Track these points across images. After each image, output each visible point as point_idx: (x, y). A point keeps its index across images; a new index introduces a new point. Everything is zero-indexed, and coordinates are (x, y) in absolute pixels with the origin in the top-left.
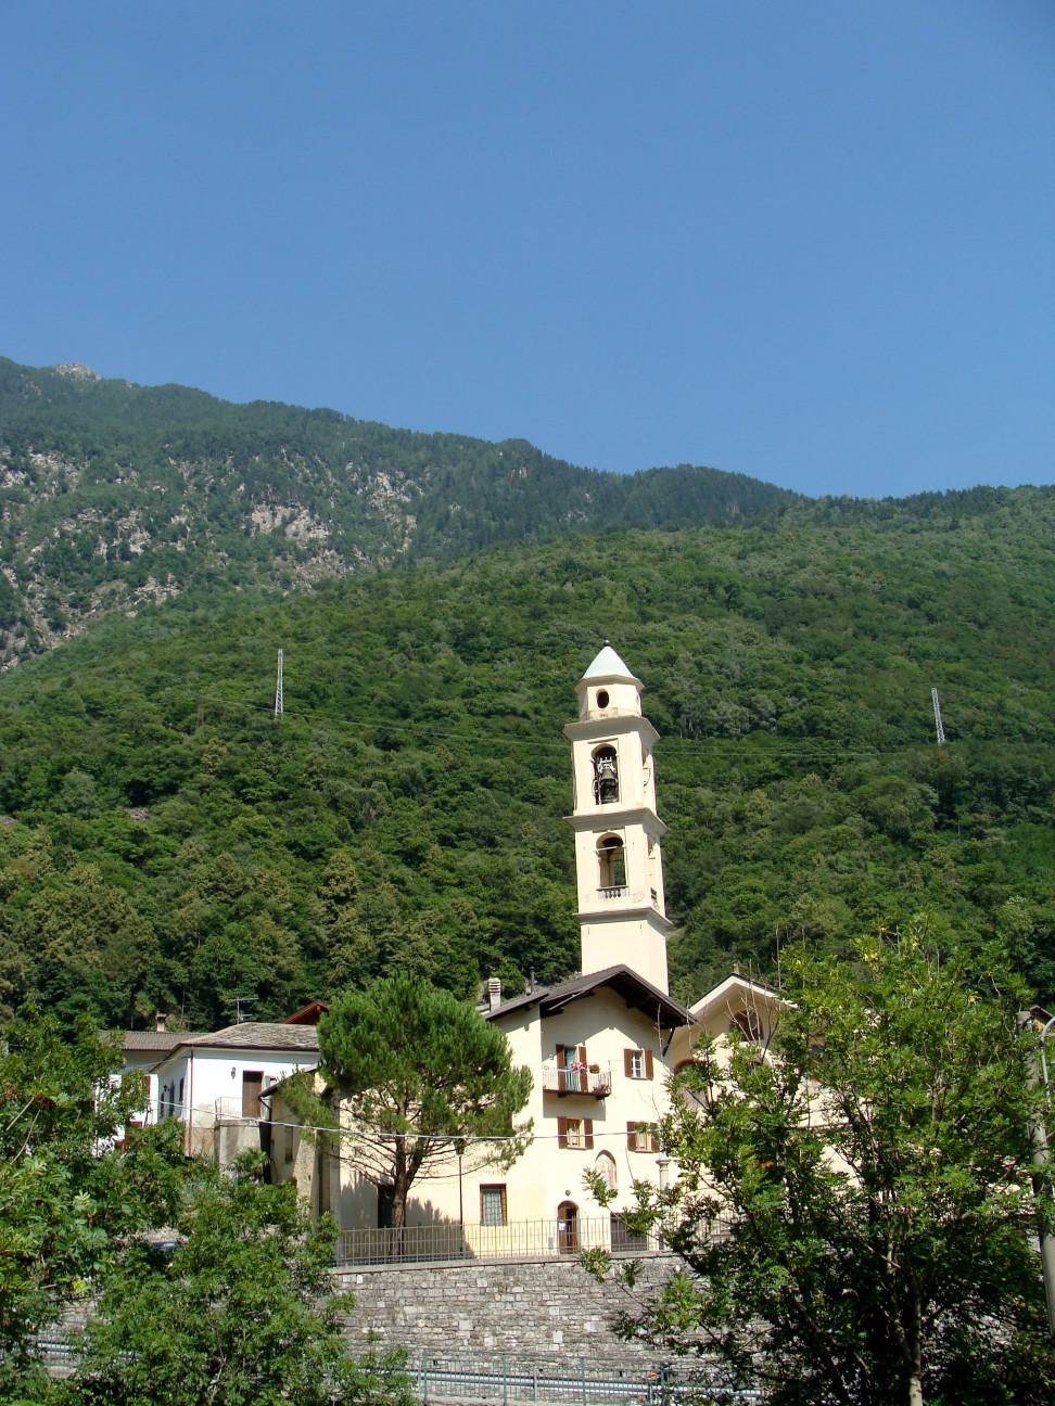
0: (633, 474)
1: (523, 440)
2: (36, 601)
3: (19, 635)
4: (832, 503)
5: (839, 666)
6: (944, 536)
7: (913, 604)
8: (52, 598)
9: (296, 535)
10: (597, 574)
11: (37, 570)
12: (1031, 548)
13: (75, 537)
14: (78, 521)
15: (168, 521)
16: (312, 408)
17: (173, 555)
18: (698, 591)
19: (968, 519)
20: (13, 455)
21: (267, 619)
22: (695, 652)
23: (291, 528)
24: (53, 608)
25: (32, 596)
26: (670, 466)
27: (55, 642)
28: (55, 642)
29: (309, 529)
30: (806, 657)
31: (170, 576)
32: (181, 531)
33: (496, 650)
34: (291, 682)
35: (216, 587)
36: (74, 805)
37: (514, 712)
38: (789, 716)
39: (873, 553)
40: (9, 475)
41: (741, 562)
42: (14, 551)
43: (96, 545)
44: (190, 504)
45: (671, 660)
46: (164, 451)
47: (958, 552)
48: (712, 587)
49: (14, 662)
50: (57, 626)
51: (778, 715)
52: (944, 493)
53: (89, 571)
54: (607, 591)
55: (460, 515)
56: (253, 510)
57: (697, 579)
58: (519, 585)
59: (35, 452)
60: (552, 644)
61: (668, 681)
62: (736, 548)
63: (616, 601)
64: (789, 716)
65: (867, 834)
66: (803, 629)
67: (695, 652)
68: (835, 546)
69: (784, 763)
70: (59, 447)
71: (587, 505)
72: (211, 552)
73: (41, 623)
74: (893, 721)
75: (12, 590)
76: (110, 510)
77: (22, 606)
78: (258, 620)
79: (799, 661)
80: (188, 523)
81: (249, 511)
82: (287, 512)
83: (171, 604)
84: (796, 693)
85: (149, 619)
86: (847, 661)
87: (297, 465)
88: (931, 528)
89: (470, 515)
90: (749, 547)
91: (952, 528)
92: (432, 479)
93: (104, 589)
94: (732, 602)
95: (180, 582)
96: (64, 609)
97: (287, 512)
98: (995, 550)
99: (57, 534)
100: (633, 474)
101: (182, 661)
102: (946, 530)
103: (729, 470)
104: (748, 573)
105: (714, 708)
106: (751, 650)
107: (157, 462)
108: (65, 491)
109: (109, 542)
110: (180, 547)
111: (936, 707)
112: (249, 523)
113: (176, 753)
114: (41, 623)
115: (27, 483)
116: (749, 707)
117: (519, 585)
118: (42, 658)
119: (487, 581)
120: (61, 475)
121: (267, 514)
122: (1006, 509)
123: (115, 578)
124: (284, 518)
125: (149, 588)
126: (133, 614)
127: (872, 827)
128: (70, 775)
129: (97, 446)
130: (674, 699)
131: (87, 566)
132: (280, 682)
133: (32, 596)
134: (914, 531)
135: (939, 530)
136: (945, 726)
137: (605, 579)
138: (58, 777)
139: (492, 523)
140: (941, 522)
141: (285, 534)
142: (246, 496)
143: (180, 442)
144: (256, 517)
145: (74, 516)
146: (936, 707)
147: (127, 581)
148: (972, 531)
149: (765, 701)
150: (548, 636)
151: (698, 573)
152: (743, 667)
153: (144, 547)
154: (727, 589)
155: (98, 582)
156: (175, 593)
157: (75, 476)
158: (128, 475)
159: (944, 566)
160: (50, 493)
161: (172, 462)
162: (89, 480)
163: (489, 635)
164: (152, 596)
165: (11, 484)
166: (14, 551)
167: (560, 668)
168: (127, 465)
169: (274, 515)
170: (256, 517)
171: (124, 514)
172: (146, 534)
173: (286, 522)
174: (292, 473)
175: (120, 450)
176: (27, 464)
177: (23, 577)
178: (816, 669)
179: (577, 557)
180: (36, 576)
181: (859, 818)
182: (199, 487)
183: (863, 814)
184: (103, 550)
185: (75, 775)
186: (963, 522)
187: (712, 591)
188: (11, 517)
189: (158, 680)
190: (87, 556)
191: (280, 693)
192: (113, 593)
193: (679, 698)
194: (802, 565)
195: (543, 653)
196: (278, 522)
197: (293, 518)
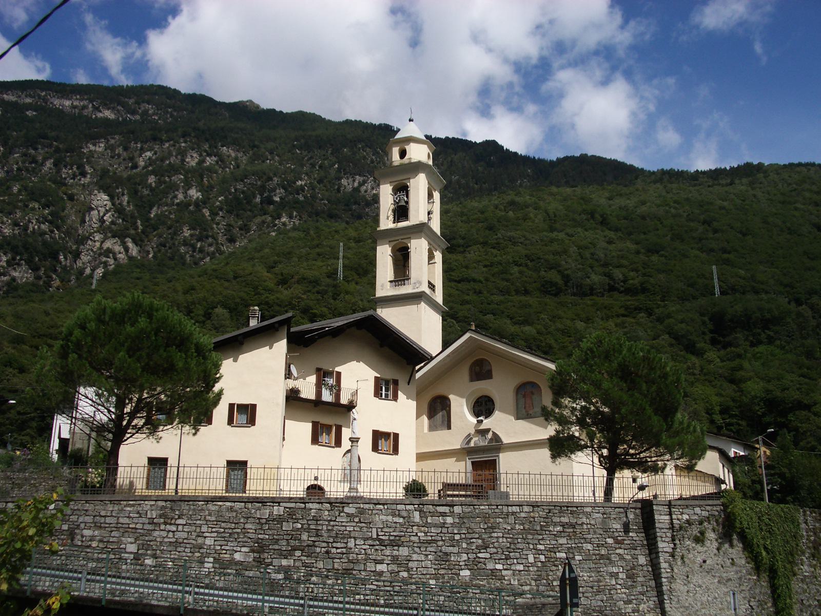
0: (555, 160)
1: (494, 141)
2: (220, 226)
3: (211, 245)
4: (663, 172)
5: (662, 256)
6: (726, 189)
7: (704, 222)
8: (229, 225)
9: (366, 191)
10: (527, 207)
11: (221, 209)
12: (775, 195)
13: (243, 192)
14: (245, 183)
15: (295, 183)
16: (377, 123)
17: (297, 202)
18: (584, 217)
19: (740, 179)
20: (210, 147)
21: (341, 231)
22: (579, 248)
23: (363, 188)
24: (230, 230)
25: (218, 224)
26: (576, 155)
27: (227, 248)
28: (227, 248)
29: (373, 189)
30: (643, 251)
31: (295, 213)
32: (302, 188)
33: (467, 247)
34: (347, 262)
35: (320, 219)
36: (217, 326)
37: (474, 280)
38: (631, 282)
39: (686, 196)
40: (208, 158)
41: (611, 202)
42: (209, 199)
43: (255, 197)
44: (307, 174)
45: (565, 252)
46: (294, 146)
47: (733, 197)
48: (592, 215)
49: (208, 259)
50: (232, 240)
51: (625, 281)
52: (728, 168)
53: (250, 211)
54: (532, 215)
55: (458, 182)
56: (342, 178)
57: (584, 210)
58: (482, 213)
59: (223, 146)
60: (498, 243)
61: (563, 263)
62: (607, 194)
63: (537, 221)
64: (631, 282)
65: (671, 345)
66: (643, 236)
67: (579, 248)
68: (664, 194)
69: (627, 308)
70: (235, 143)
71: (528, 176)
72: (318, 201)
73: (221, 239)
74: (691, 285)
75: (207, 220)
76: (262, 177)
77: (212, 228)
78: (336, 232)
79: (638, 252)
80: (305, 185)
81: (340, 179)
82: (361, 179)
83: (295, 229)
84: (637, 271)
85: (282, 236)
86: (667, 254)
87: (367, 154)
88: (720, 184)
89: (463, 181)
90: (615, 194)
91: (731, 184)
92: (443, 162)
93: (258, 220)
94: (604, 222)
95: (300, 217)
96: (236, 231)
97: (361, 179)
98: (755, 196)
99: (233, 190)
100: (555, 160)
101: (289, 253)
102: (727, 185)
103: (608, 157)
104: (613, 207)
105: (589, 278)
106: (611, 247)
107: (289, 152)
108: (238, 167)
109: (261, 195)
110: (301, 198)
111: (715, 277)
112: (340, 185)
113: (278, 299)
114: (221, 239)
115: (217, 162)
116: (608, 276)
117: (482, 213)
118: (223, 257)
119: (465, 211)
120: (236, 159)
121: (351, 180)
122: (762, 175)
123: (265, 214)
124: (359, 182)
125: (284, 220)
126: (274, 234)
127: (674, 342)
128: (216, 310)
129: (256, 143)
130: (566, 272)
131: (249, 208)
132: (341, 261)
133: (218, 224)
134: (709, 186)
135: (723, 186)
136: (720, 287)
137: (531, 209)
138: (210, 311)
139: (476, 186)
140: (724, 182)
141: (360, 191)
142: (339, 170)
143: (303, 141)
144: (344, 182)
145: (242, 181)
146: (715, 277)
147: (271, 216)
148: (741, 186)
149: (618, 274)
150: (497, 239)
151: (584, 207)
152: (606, 255)
153: (281, 198)
154: (602, 216)
155: (255, 216)
156: (297, 223)
157: (244, 159)
158: (273, 159)
159: (725, 204)
160: (230, 168)
161: (298, 151)
162: (252, 161)
163: (463, 238)
164: (284, 224)
165: (208, 163)
166: (209, 199)
167: (501, 256)
168: (273, 153)
169: (354, 181)
170: (344, 182)
171: (270, 179)
172: (282, 191)
173: (361, 184)
174: (364, 158)
175: (270, 145)
176: (217, 152)
177: (214, 214)
178: (648, 257)
179: (517, 199)
180: (221, 213)
181: (667, 336)
182: (313, 166)
183: (669, 333)
184: (258, 199)
185: (219, 310)
186: (737, 181)
187: (593, 217)
188: (208, 181)
189: (275, 262)
190: (249, 203)
191: (340, 269)
192: (264, 222)
193: (569, 272)
194: (643, 203)
195: (494, 248)
196: (356, 184)
197: (364, 182)
